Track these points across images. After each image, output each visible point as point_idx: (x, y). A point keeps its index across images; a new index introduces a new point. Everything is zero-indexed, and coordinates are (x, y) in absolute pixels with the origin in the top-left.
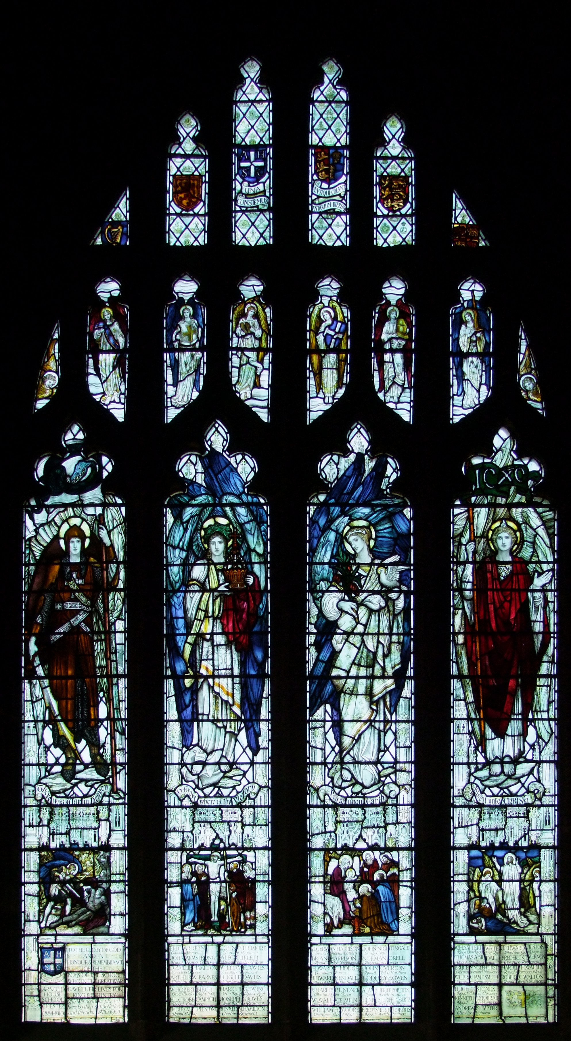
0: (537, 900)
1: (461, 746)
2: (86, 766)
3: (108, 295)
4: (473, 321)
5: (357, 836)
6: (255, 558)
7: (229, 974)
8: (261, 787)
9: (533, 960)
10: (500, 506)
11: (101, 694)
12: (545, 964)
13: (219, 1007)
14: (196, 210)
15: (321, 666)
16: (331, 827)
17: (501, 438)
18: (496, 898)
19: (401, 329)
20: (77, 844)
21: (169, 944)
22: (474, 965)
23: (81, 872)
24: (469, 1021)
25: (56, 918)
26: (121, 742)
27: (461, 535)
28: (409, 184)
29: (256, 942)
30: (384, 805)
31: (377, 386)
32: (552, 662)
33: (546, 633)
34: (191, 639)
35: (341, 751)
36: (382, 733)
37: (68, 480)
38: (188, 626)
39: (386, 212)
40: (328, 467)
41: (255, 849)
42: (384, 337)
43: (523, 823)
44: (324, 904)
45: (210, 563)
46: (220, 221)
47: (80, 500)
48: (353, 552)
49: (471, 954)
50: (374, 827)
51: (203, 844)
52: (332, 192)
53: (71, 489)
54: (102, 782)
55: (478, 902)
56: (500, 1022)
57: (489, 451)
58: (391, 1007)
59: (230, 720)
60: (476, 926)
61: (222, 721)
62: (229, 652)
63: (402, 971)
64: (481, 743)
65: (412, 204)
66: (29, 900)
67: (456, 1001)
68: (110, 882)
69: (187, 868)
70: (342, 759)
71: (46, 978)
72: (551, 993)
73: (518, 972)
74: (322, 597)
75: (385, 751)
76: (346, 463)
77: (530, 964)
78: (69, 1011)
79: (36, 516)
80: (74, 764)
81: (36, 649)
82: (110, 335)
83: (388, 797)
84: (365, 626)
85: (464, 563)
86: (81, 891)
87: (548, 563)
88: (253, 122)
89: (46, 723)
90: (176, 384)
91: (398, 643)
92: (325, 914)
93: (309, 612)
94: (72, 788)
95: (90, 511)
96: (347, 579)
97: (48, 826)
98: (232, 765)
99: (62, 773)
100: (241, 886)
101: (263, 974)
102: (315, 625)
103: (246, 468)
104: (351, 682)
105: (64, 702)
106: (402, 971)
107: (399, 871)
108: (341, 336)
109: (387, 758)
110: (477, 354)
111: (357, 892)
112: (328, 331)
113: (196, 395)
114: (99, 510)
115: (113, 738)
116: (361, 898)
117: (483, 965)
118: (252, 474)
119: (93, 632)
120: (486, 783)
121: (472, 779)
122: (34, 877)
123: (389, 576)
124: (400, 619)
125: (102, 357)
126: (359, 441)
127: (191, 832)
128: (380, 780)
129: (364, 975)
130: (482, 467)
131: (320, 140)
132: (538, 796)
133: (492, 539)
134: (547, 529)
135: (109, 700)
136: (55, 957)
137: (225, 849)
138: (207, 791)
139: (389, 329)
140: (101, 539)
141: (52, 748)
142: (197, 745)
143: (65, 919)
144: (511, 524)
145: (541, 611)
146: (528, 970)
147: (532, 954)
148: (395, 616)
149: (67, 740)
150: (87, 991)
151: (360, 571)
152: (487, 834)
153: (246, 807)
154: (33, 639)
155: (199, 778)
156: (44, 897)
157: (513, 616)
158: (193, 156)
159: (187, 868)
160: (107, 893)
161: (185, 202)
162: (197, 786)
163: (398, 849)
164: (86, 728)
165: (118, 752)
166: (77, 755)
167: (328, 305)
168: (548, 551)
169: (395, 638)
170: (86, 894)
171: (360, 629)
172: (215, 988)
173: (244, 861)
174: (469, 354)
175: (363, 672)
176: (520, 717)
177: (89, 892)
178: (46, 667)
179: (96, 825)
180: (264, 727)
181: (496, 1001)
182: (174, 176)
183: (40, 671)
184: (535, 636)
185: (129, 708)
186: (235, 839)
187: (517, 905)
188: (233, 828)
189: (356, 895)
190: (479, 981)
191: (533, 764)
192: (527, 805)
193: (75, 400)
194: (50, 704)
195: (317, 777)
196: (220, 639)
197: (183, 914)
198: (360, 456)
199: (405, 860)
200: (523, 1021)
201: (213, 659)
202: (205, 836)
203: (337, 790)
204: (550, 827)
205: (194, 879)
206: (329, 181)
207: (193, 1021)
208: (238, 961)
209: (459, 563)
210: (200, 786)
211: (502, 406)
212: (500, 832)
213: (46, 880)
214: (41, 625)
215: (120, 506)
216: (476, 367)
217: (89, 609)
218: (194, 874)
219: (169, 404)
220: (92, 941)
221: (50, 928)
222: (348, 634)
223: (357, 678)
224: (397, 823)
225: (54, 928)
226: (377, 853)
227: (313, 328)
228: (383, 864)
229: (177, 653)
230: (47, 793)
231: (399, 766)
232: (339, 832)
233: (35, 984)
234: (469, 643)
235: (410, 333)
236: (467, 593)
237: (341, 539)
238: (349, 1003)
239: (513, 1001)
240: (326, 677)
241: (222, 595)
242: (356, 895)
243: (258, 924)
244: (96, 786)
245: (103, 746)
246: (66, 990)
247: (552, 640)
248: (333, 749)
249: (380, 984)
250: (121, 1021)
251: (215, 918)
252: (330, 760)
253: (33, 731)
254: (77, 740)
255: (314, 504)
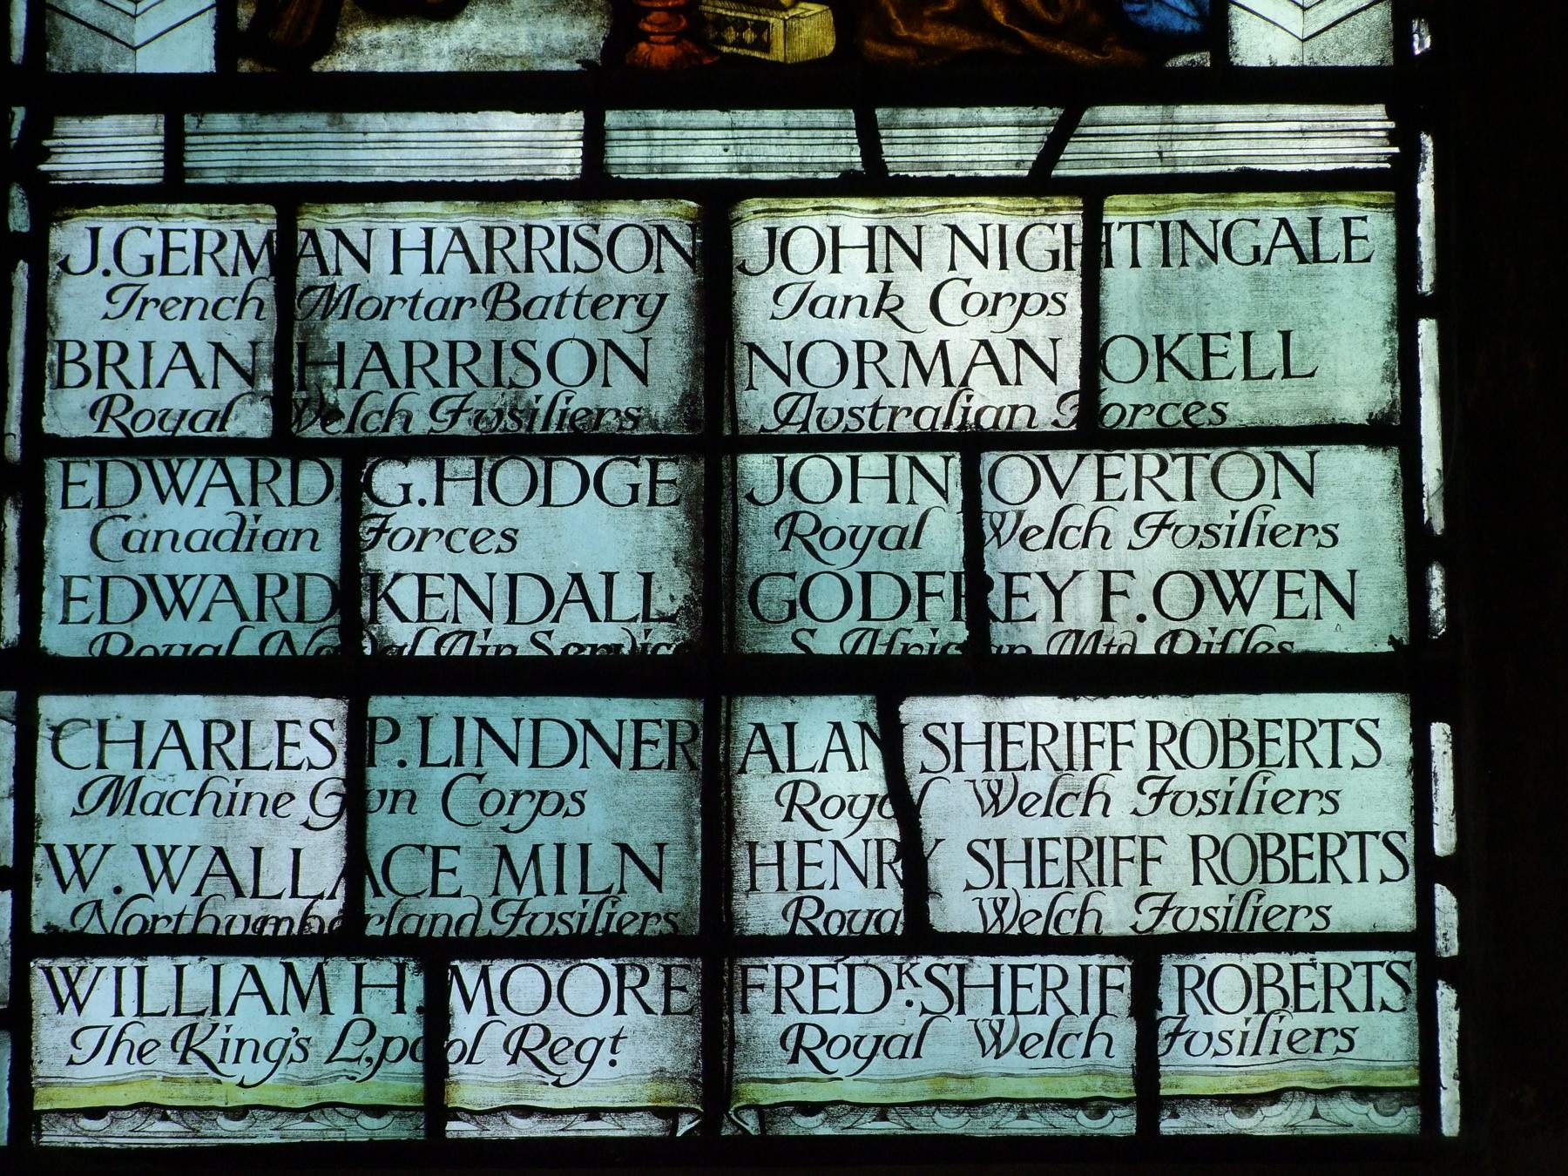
58: (1145, 953)
63: (1289, 507)
106: (1289, 507)
129: (760, 549)
238: (552, 907)
249: (986, 669)
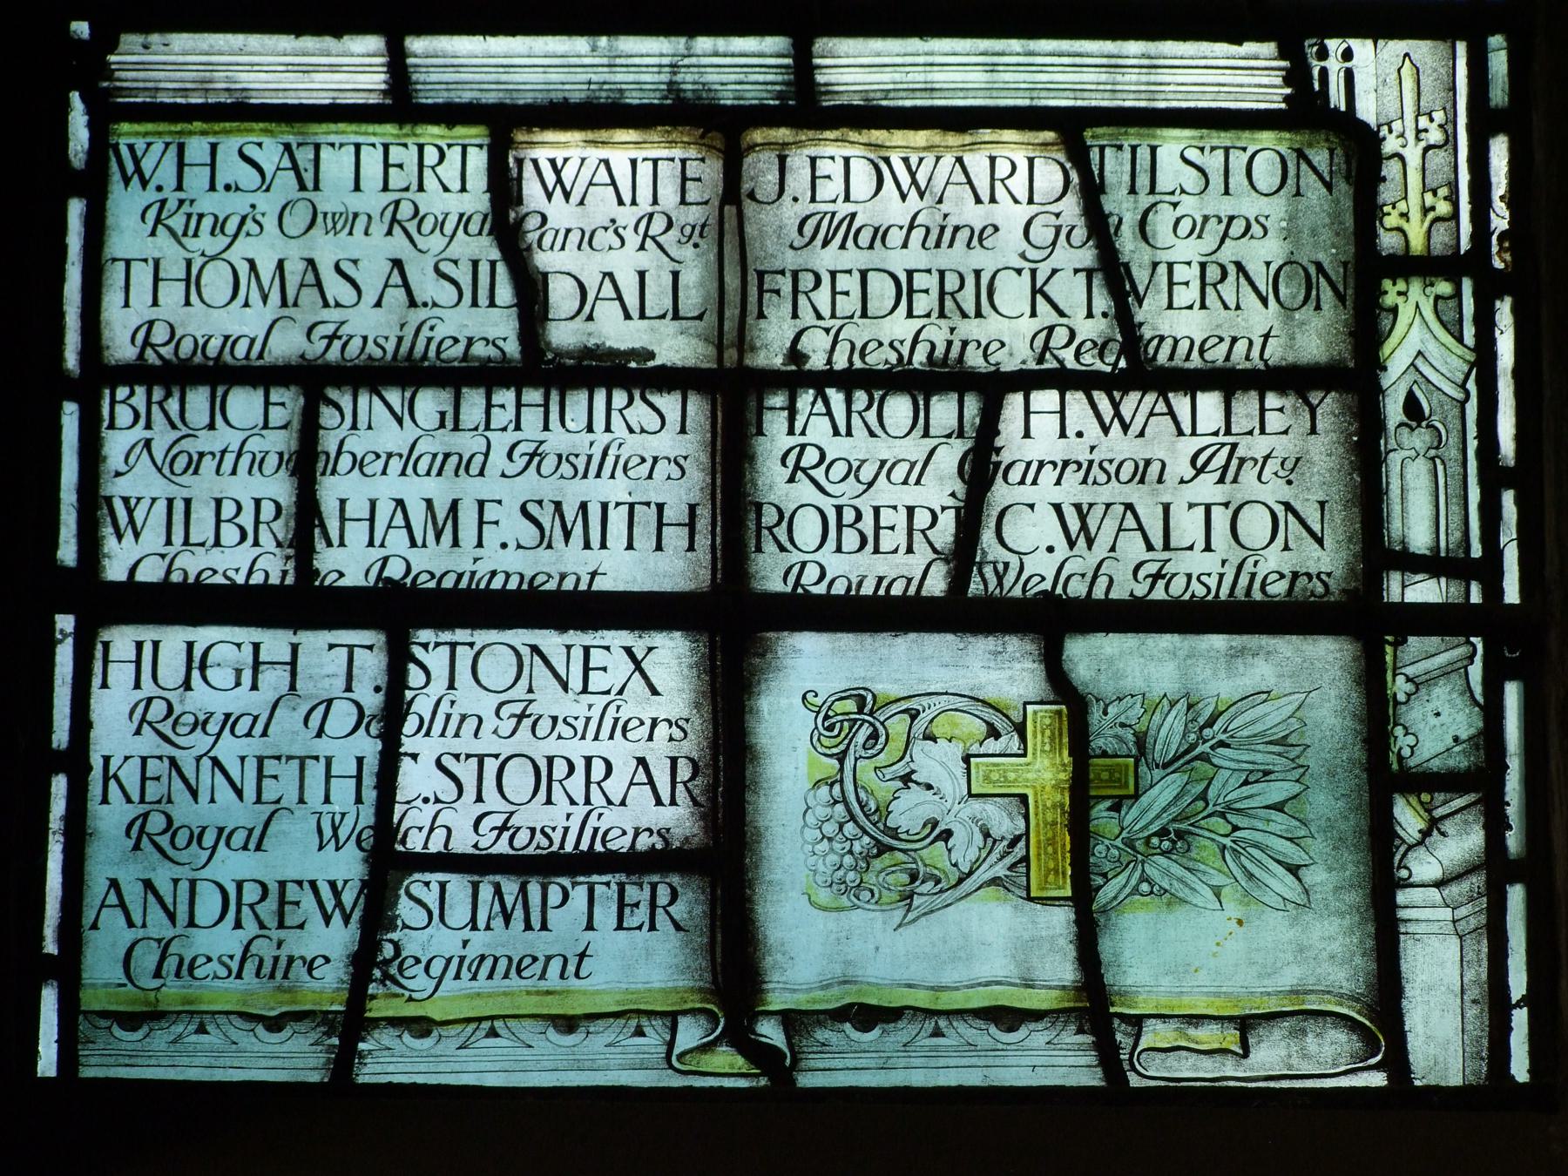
9: (1178, 324)
12: (1353, 377)
22: (371, 375)
24: (295, 1059)
49: (327, 249)
56: (726, 1068)
67: (110, 818)
72: (1436, 726)
73: (981, 468)
117: (487, 375)
146: (1119, 445)
200: (1056, 1061)
239: (909, 812)
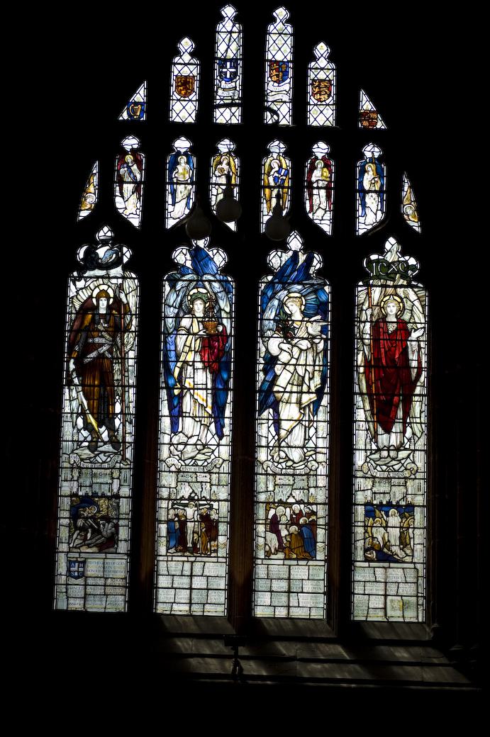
0: (412, 540)
1: (361, 438)
2: (105, 443)
3: (131, 147)
4: (373, 171)
5: (288, 494)
6: (224, 315)
7: (199, 583)
8: (224, 460)
9: (408, 580)
10: (389, 286)
11: (117, 397)
12: (417, 583)
13: (190, 604)
14: (190, 97)
15: (267, 384)
16: (271, 488)
17: (391, 243)
18: (383, 538)
19: (325, 174)
20: (97, 493)
21: (158, 561)
23: (99, 511)
24: (364, 619)
25: (80, 542)
26: (130, 428)
27: (363, 304)
28: (331, 85)
29: (217, 562)
30: (307, 474)
31: (308, 209)
32: (424, 386)
33: (420, 368)
34: (179, 364)
35: (279, 439)
36: (307, 429)
37: (100, 261)
38: (178, 356)
39: (316, 102)
40: (274, 259)
41: (219, 501)
42: (314, 179)
43: (403, 489)
44: (265, 538)
45: (194, 317)
46: (207, 104)
47: (107, 274)
48: (290, 313)
50: (300, 489)
51: (183, 496)
52: (281, 88)
53: (101, 267)
54: (115, 454)
55: (371, 540)
56: (385, 620)
57: (381, 251)
59: (204, 417)
60: (369, 556)
61: (199, 417)
62: (205, 373)
64: (375, 437)
65: (333, 97)
66: (62, 528)
67: (355, 605)
68: (118, 519)
69: (172, 512)
70: (280, 444)
71: (73, 581)
74: (268, 341)
75: (309, 440)
76: (286, 257)
77: (406, 583)
78: (87, 602)
79: (77, 283)
80: (97, 442)
81: (74, 367)
82: (131, 172)
83: (311, 470)
84: (297, 359)
85: (365, 322)
86: (98, 524)
87: (421, 323)
88: (228, 42)
89: (78, 415)
90: (174, 204)
91: (319, 371)
92: (266, 544)
93: (259, 350)
94: (95, 457)
95: (114, 281)
96: (285, 329)
97: (77, 481)
98: (205, 446)
99: (88, 447)
100: (210, 526)
101: (222, 584)
102: (263, 358)
103: (219, 258)
104: (286, 395)
105: (92, 402)
107: (317, 518)
108: (284, 178)
109: (311, 444)
110: (375, 192)
111: (288, 531)
112: (276, 174)
113: (187, 211)
114: (120, 281)
115: (124, 426)
116: (290, 535)
118: (224, 262)
119: (113, 358)
120: (377, 463)
121: (368, 460)
122: (67, 514)
123: (314, 329)
124: (321, 355)
125: (125, 186)
126: (295, 243)
127: (175, 488)
128: (305, 458)
130: (377, 261)
131: (274, 57)
132: (413, 472)
133: (383, 307)
134: (421, 302)
135: (122, 401)
136: (79, 567)
137: (198, 500)
138: (187, 462)
139: (316, 175)
140: (121, 299)
141: (82, 431)
142: (181, 432)
143: (86, 542)
144: (396, 298)
145: (416, 354)
147: (408, 575)
148: (318, 354)
149: (93, 426)
150: (99, 590)
151: (295, 325)
152: (377, 496)
153: (213, 473)
154: (72, 361)
155: (182, 453)
156: (73, 527)
157: (397, 356)
158: (189, 64)
159: (172, 512)
160: (117, 527)
161: (183, 92)
162: (181, 459)
163: (317, 504)
164: (105, 418)
165: (127, 435)
166: (99, 436)
167: (276, 159)
168: (421, 316)
169: (317, 368)
170: (102, 526)
171: (294, 361)
172: (188, 591)
173: (211, 508)
174: (370, 191)
175: (295, 389)
176: (401, 421)
177: (104, 525)
178: (81, 378)
179: (110, 481)
180: (227, 422)
181: (382, 606)
182: (176, 76)
183: (76, 381)
184: (412, 370)
185: (137, 407)
186: (205, 494)
187: (398, 543)
188: (204, 487)
189: (287, 533)
190: (370, 592)
191: (410, 452)
192: (405, 478)
193: (106, 212)
194: (82, 402)
195: (262, 455)
196: (199, 365)
197: (168, 542)
198: (296, 253)
199: (322, 511)
200: (401, 620)
201: (194, 378)
202: (185, 491)
203: (276, 464)
204: (421, 493)
205: (176, 519)
206: (278, 82)
207: (173, 613)
208: (205, 574)
209: (360, 322)
210: (183, 458)
211: (392, 223)
212: (387, 495)
213: (75, 516)
214: (78, 352)
215: (134, 279)
216: (374, 199)
217: (111, 343)
218: (176, 515)
219: (169, 216)
220: (104, 557)
221: (76, 548)
222: (285, 364)
223: (291, 392)
224: (316, 487)
225: (79, 548)
226: (302, 506)
227: (266, 172)
228: (306, 513)
229: (169, 373)
230: (77, 459)
231: (318, 450)
232: (277, 490)
233: (64, 585)
234: (367, 372)
235: (331, 177)
236: (366, 341)
237: (282, 304)
240: (270, 391)
241: (201, 337)
242: (287, 533)
243: (219, 549)
244: (111, 456)
245: (117, 431)
246: (85, 589)
247: (423, 372)
248: (274, 437)
249: (302, 592)
250: (123, 610)
251: (190, 545)
252: (271, 444)
253: (69, 419)
254: (100, 426)
255: (264, 282)
